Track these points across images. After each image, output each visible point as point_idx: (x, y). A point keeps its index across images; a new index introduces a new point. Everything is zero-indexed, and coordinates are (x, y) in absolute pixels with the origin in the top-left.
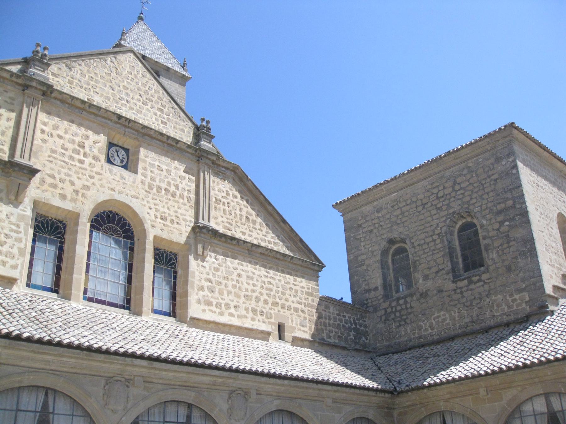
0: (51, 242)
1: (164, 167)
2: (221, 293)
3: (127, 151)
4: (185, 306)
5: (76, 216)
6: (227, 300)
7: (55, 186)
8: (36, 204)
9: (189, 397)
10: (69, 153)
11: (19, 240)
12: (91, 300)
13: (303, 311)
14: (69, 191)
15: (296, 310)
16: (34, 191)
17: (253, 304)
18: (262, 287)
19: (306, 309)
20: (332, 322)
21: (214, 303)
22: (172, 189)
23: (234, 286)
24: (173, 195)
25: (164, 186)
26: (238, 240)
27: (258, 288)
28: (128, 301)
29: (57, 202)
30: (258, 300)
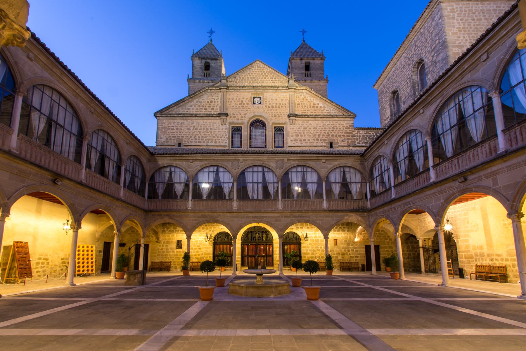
0: (238, 134)
1: (274, 99)
2: (301, 136)
3: (260, 98)
4: (287, 143)
5: (242, 123)
6: (304, 138)
7: (235, 117)
8: (230, 123)
9: (260, 163)
10: (238, 105)
11: (226, 135)
12: (253, 148)
13: (343, 136)
14: (239, 117)
15: (340, 136)
16: (229, 120)
17: (317, 137)
18: (321, 131)
19: (346, 135)
20: (361, 137)
21: (299, 139)
22: (278, 105)
23: (307, 133)
24: (279, 107)
25: (274, 105)
26: (308, 116)
27: (319, 132)
28: (266, 146)
29: (236, 121)
30: (319, 135)
